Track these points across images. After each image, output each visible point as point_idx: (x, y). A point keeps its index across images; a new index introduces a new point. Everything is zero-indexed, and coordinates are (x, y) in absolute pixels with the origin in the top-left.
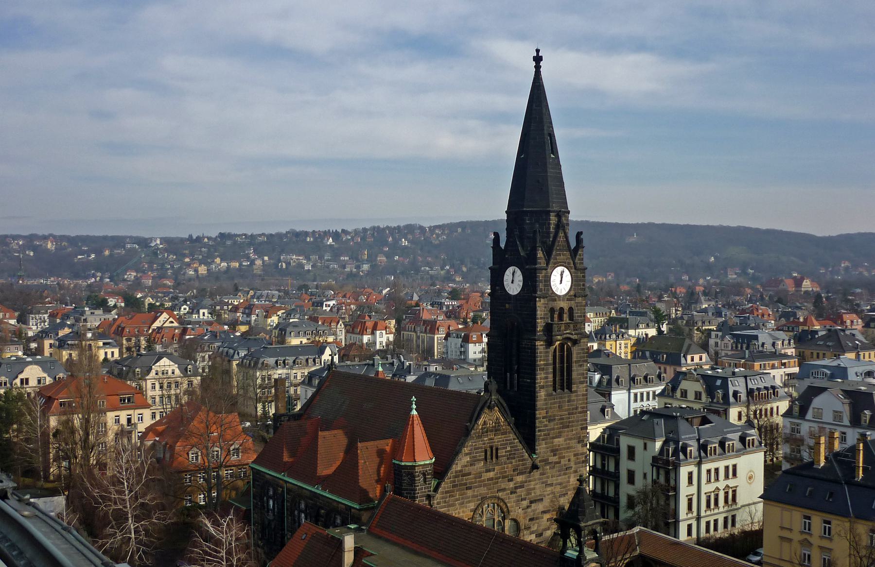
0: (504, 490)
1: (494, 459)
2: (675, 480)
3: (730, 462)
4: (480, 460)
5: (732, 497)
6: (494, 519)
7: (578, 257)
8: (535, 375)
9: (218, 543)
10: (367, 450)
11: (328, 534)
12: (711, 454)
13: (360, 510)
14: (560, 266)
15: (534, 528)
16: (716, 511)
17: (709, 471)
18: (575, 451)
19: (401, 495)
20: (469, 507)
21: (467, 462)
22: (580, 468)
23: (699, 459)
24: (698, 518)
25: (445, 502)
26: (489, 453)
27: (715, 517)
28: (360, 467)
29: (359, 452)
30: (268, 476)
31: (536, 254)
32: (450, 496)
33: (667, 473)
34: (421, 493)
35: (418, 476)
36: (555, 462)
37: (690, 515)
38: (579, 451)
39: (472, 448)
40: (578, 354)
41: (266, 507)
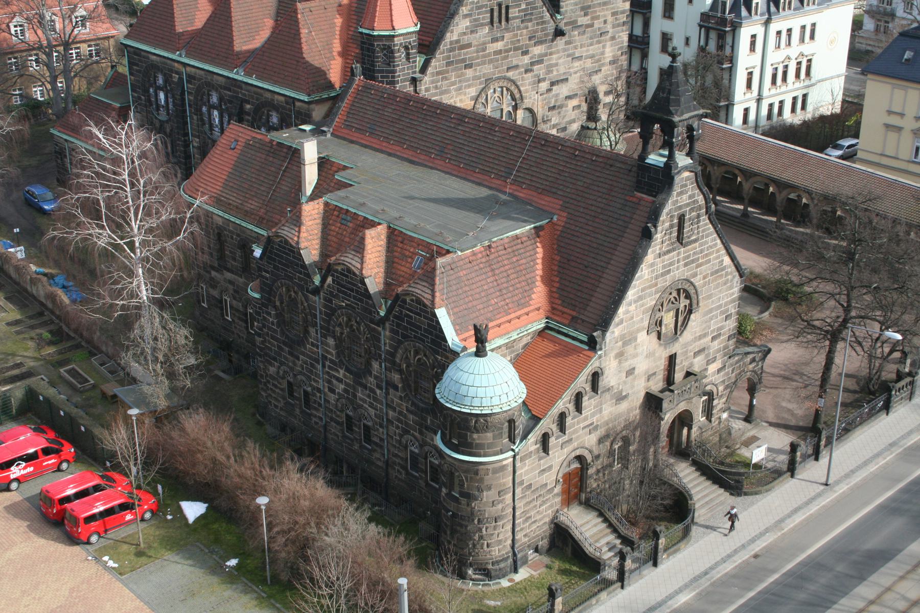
0: (517, 67)
1: (503, 23)
2: (732, 47)
3: (807, 21)
4: (482, 25)
5: (805, 69)
6: (502, 110)
9: (117, 161)
10: (310, 13)
11: (272, 141)
12: (784, 9)
13: (309, 103)
15: (554, 120)
16: (784, 89)
17: (779, 33)
18: (613, 8)
19: (373, 78)
21: (467, 28)
22: (618, 32)
23: (767, 17)
24: (759, 100)
25: (436, 87)
26: (496, 14)
27: (781, 98)
28: (303, 40)
29: (299, 16)
30: (154, 57)
32: (443, 79)
33: (721, 36)
34: (403, 75)
35: (399, 51)
37: (748, 95)
38: (618, 7)
39: (473, 7)
41: (154, 103)
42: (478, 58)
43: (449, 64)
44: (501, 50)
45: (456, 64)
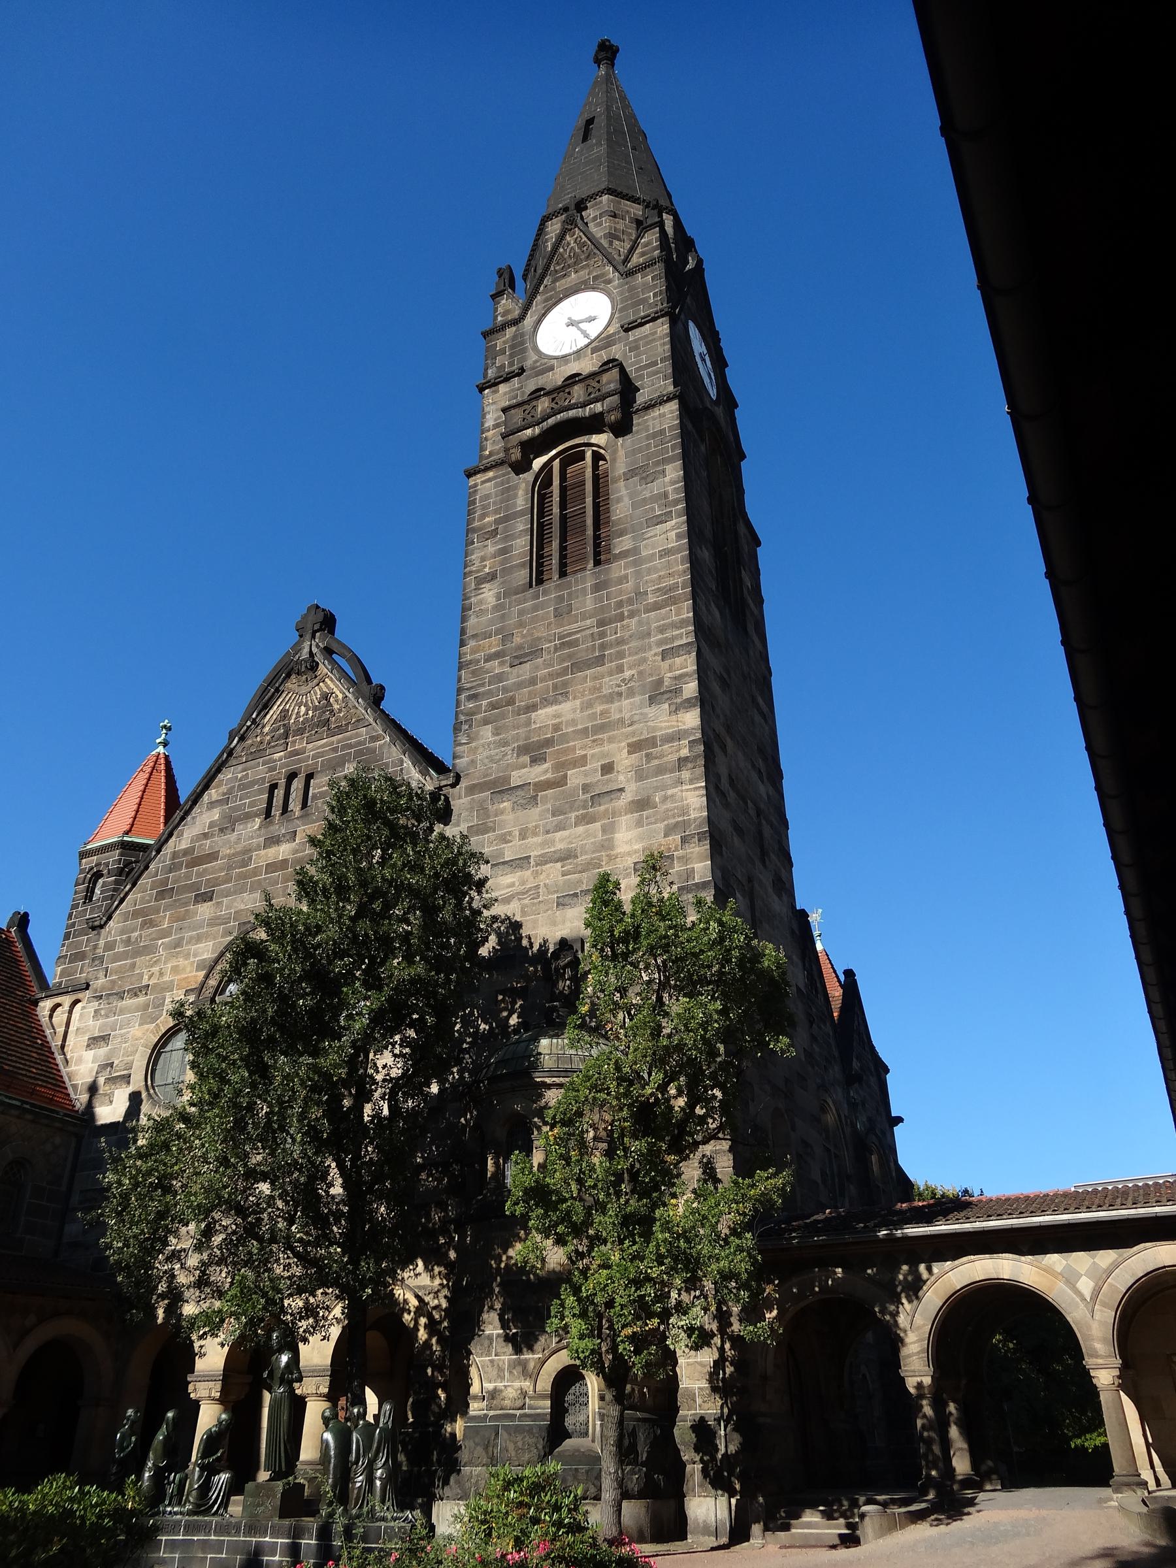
18: (633, 734)
20: (195, 955)
21: (212, 825)
22: (664, 787)
25: (128, 942)
32: (144, 924)
36: (535, 784)
38: (654, 729)
42: (228, 880)
43: (161, 895)
44: (285, 861)
45: (178, 894)
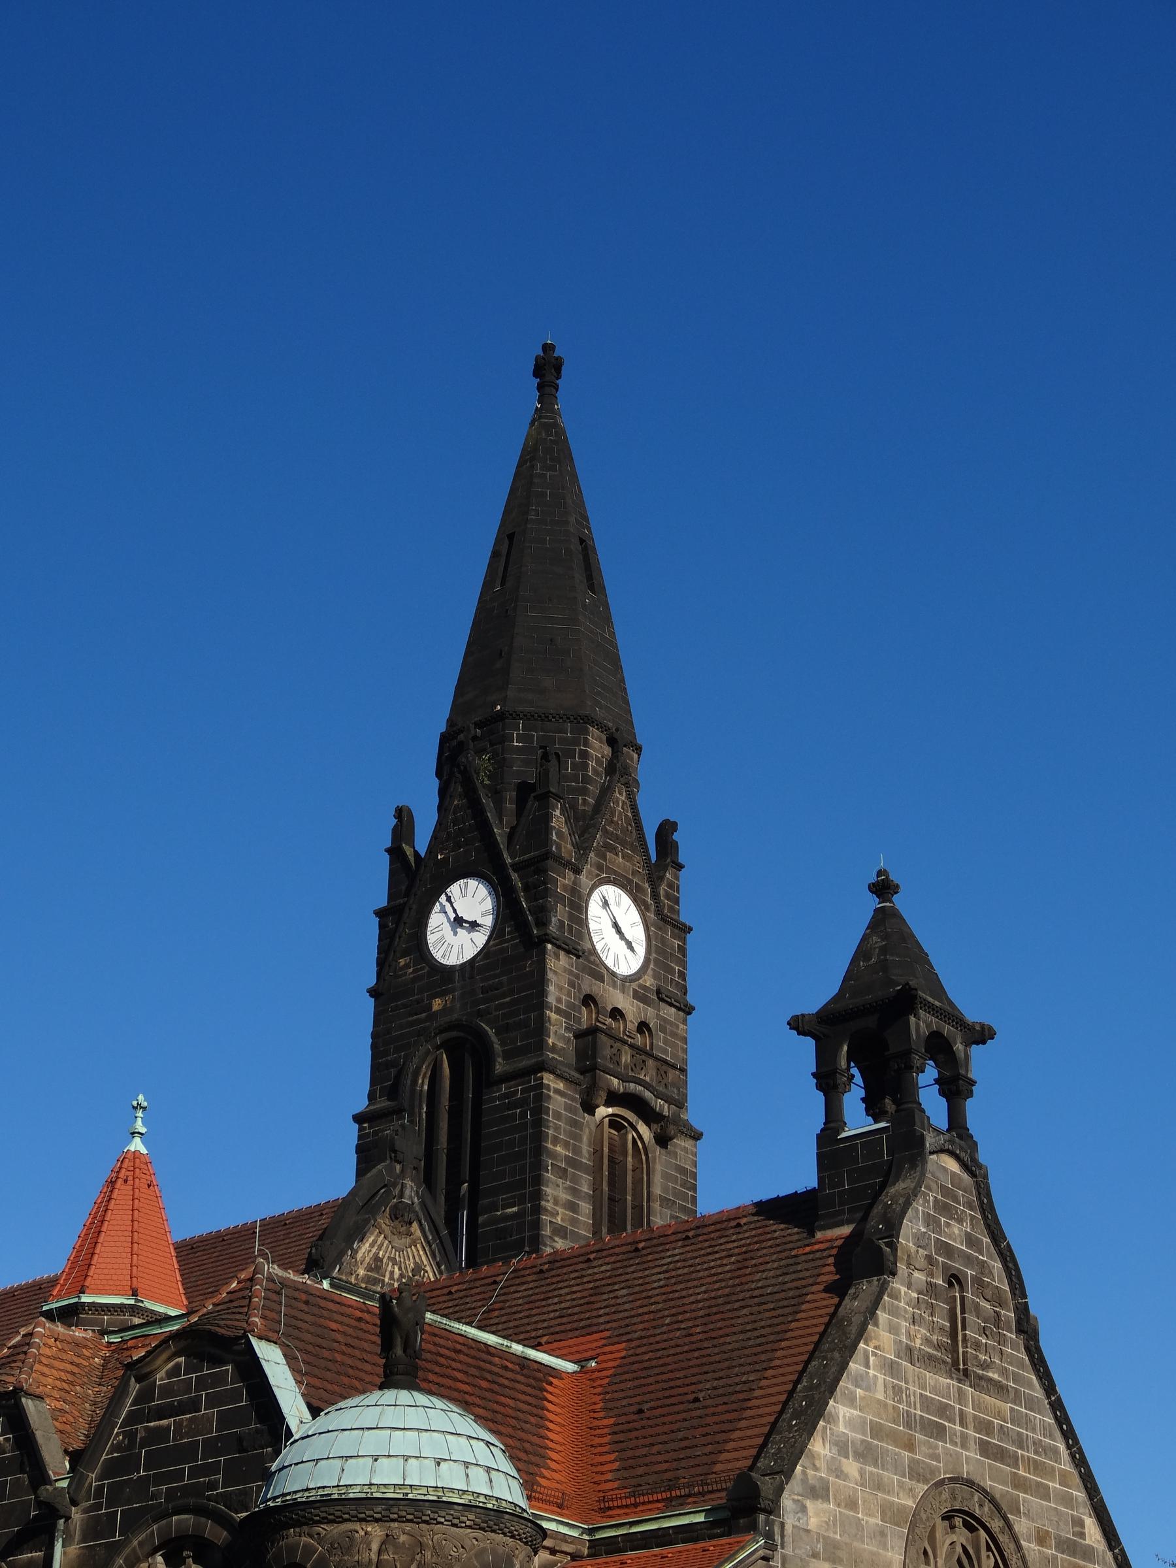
7: (664, 886)
8: (538, 1181)
14: (614, 883)
31: (547, 818)
40: (666, 1176)
